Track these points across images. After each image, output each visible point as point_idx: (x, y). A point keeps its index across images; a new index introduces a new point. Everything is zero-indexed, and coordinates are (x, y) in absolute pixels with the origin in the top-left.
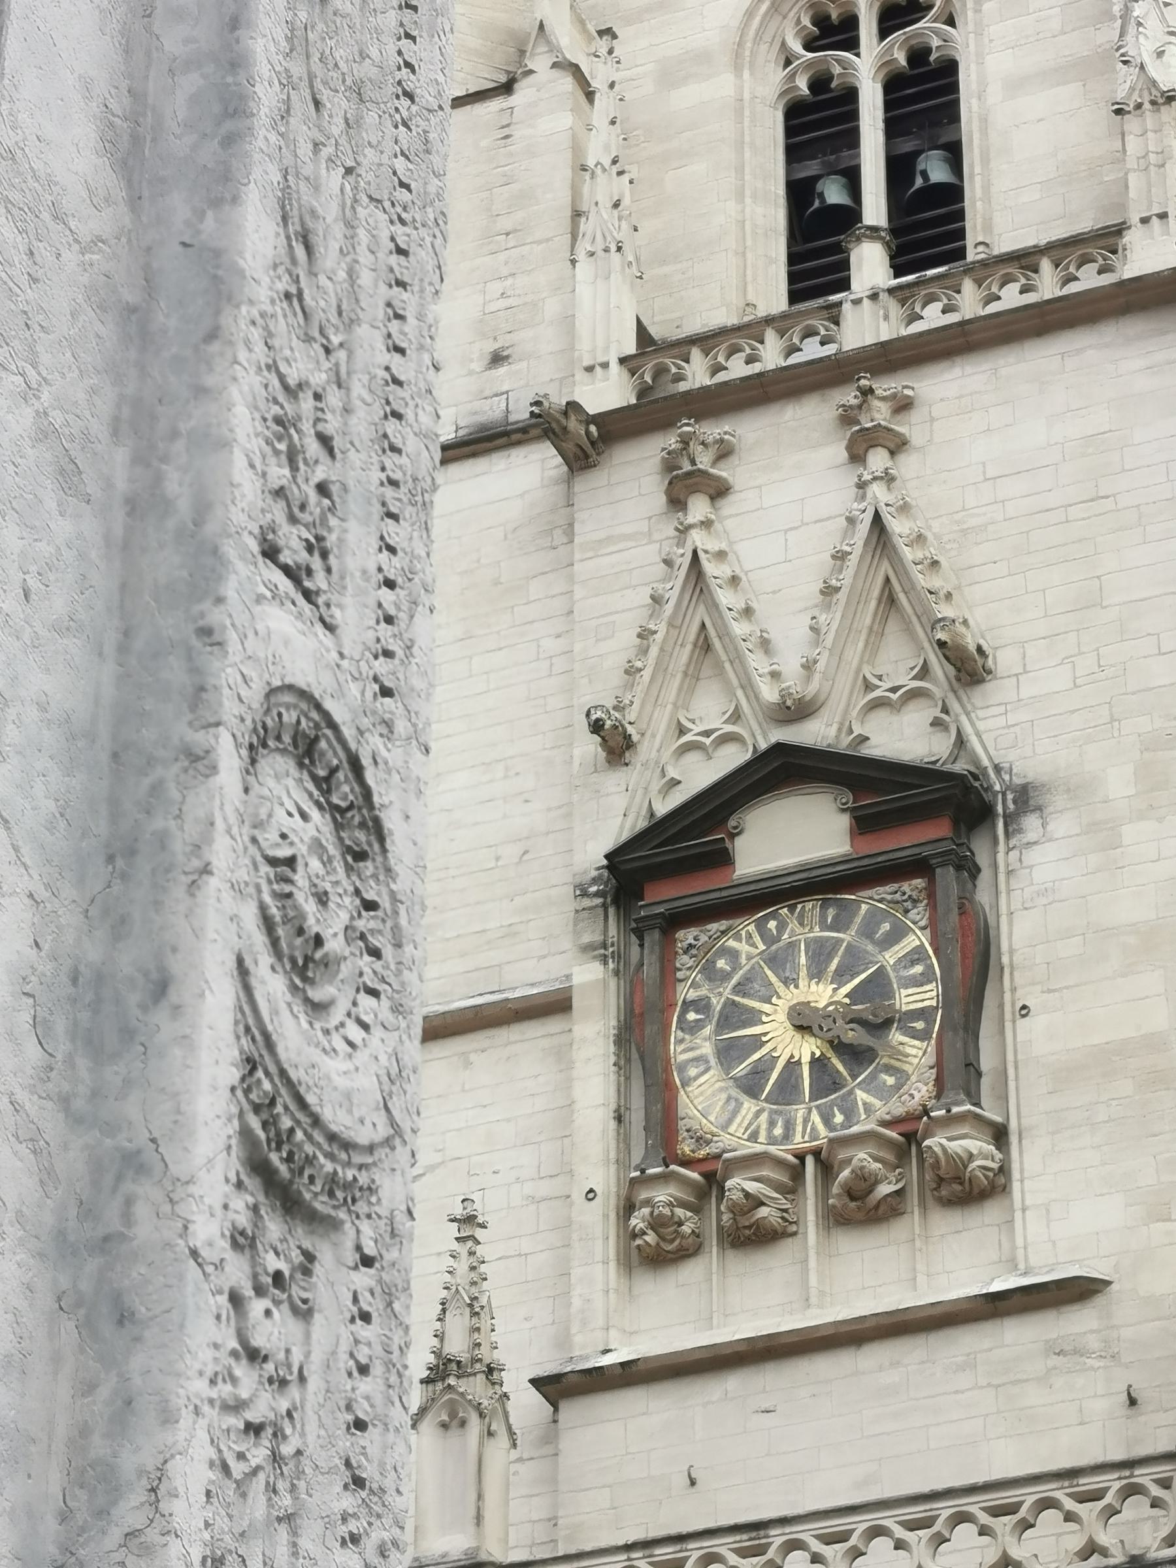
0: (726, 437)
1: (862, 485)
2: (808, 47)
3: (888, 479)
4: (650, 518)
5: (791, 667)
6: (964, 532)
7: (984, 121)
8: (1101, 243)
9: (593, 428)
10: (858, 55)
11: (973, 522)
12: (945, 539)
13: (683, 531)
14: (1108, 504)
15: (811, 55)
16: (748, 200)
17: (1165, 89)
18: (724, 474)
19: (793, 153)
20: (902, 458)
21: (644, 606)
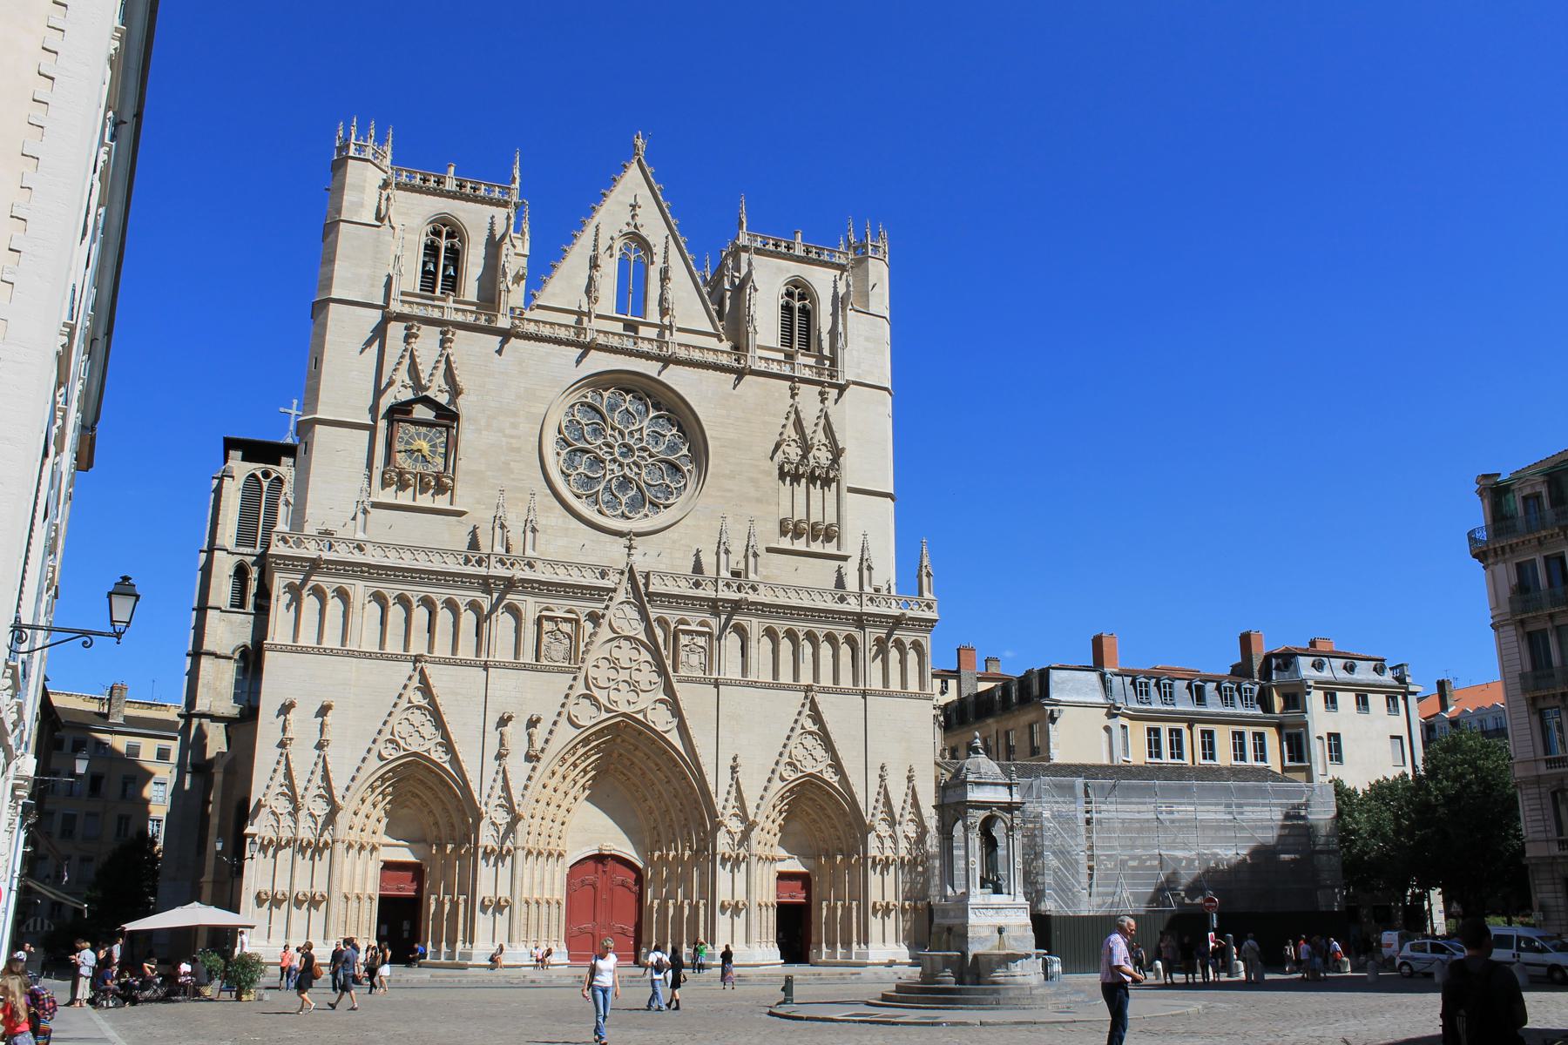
19: (425, 254)
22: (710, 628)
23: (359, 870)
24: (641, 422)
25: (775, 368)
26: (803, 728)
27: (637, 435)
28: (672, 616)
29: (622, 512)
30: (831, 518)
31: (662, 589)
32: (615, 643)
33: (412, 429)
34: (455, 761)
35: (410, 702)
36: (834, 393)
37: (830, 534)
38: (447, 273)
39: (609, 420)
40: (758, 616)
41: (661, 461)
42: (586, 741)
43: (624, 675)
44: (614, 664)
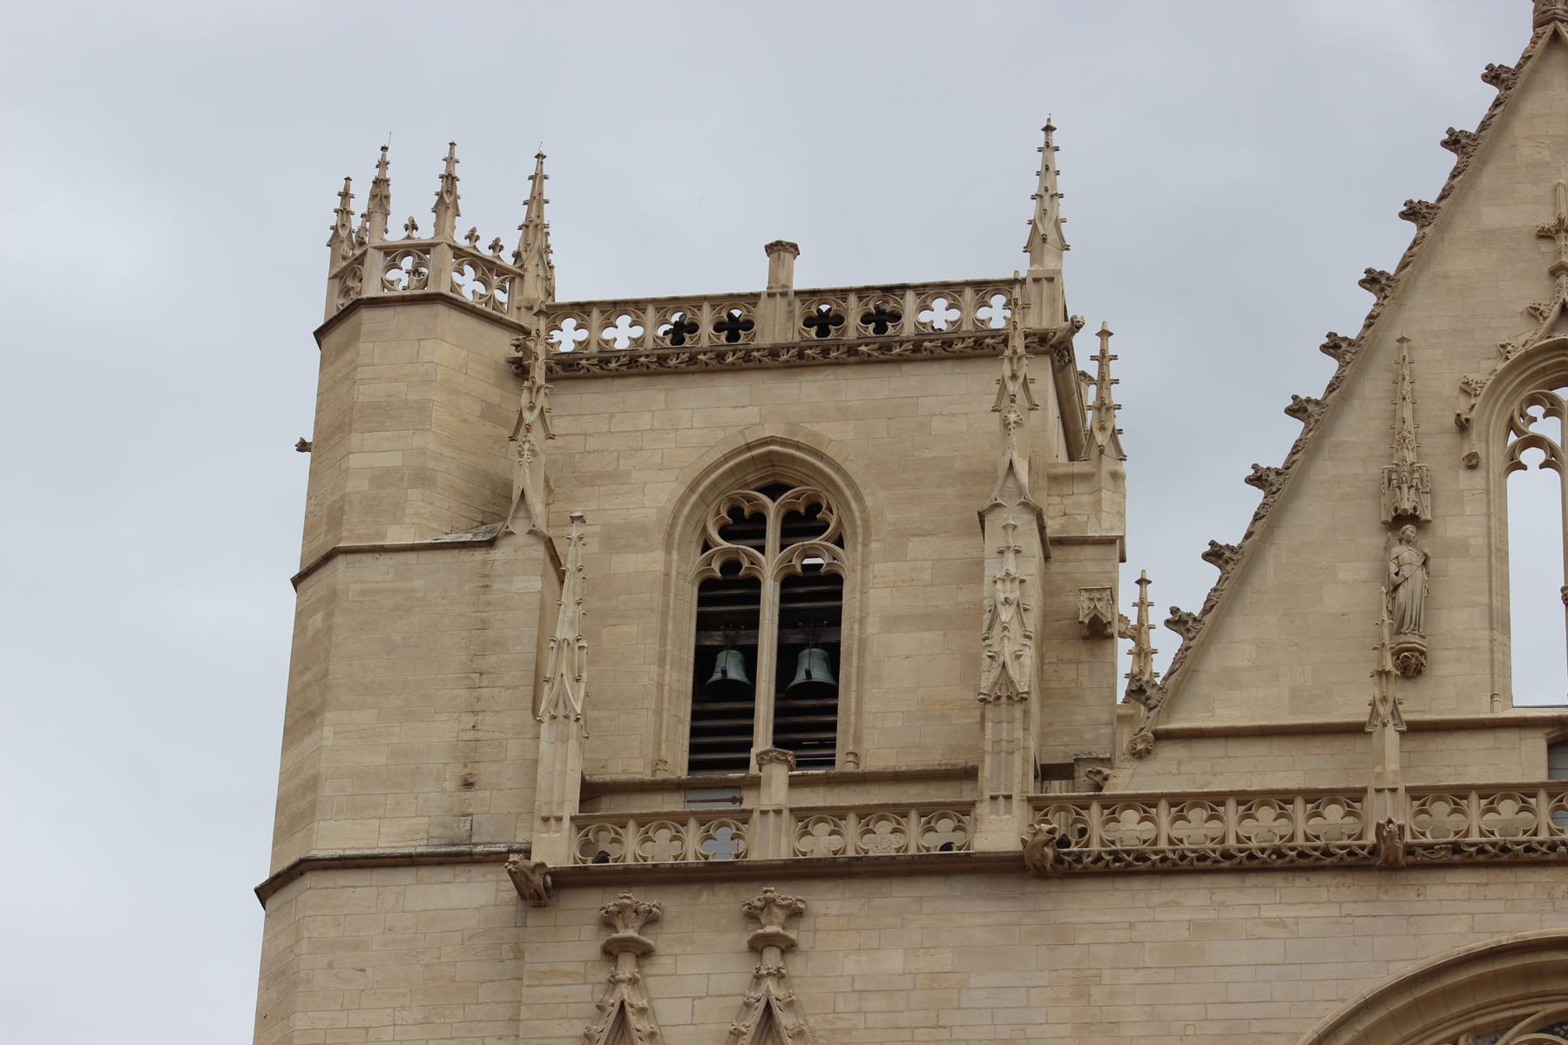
0: (654, 909)
1: (758, 978)
2: (725, 533)
3: (779, 976)
4: (586, 962)
6: (834, 1031)
7: (862, 643)
8: (958, 808)
9: (549, 879)
10: (762, 549)
11: (840, 1025)
12: (818, 1033)
13: (614, 983)
14: (945, 1034)
15: (726, 545)
16: (668, 667)
17: (1021, 691)
18: (650, 942)
19: (704, 623)
20: (790, 958)
21: (576, 1037)
38: (800, 677)
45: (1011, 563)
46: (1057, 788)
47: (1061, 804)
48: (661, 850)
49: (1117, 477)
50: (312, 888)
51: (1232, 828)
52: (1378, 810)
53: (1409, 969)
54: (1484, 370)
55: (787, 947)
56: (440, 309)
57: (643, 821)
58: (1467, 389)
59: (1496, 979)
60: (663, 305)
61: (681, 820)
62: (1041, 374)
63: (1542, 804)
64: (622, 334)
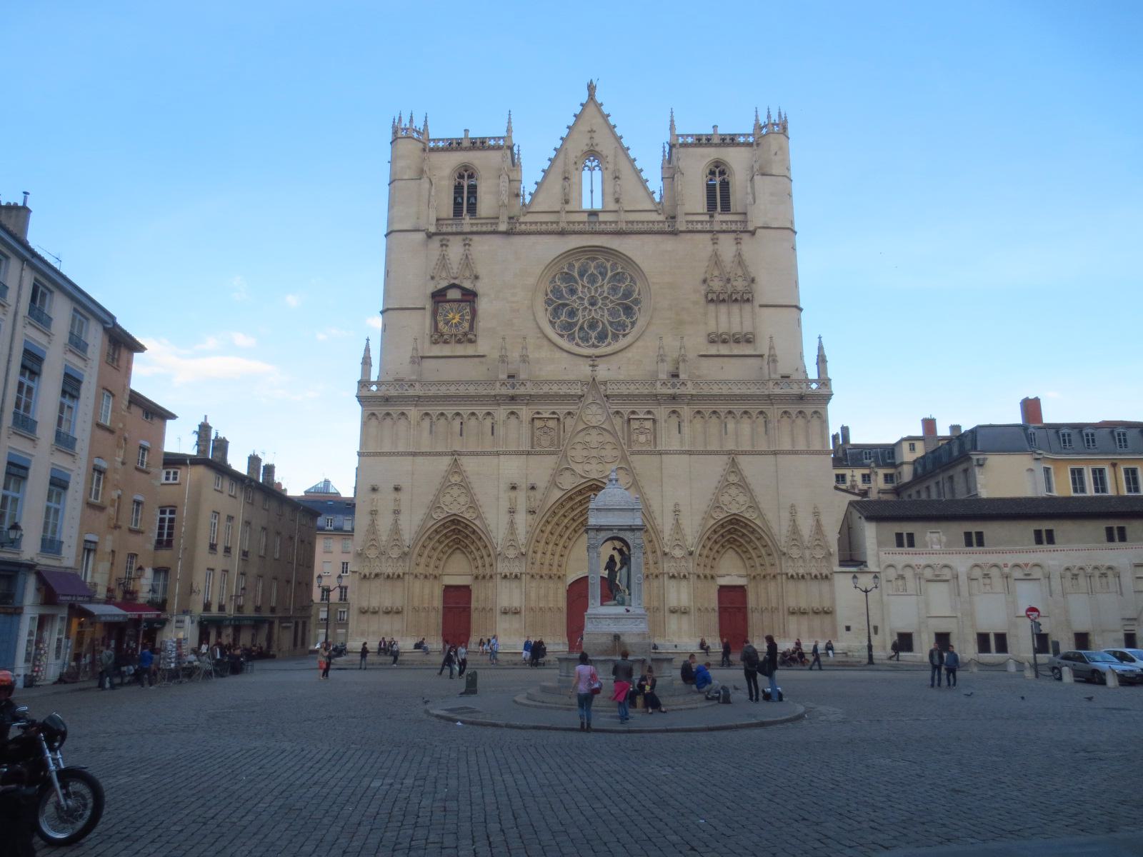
3: (469, 250)
5: (455, 271)
13: (442, 251)
19: (455, 193)
22: (654, 414)
23: (427, 591)
24: (603, 280)
25: (699, 227)
26: (727, 481)
27: (600, 290)
28: (626, 410)
29: (593, 343)
30: (747, 328)
31: (616, 392)
32: (584, 432)
33: (447, 306)
34: (479, 517)
35: (450, 481)
36: (745, 237)
37: (749, 341)
39: (580, 282)
40: (688, 404)
41: (618, 304)
42: (571, 498)
43: (594, 453)
44: (586, 446)
45: (504, 184)
46: (512, 221)
47: (512, 223)
48: (449, 230)
49: (521, 170)
50: (394, 235)
51: (539, 228)
52: (561, 225)
53: (566, 250)
54: (579, 154)
55: (469, 245)
56: (411, 139)
57: (446, 224)
58: (576, 157)
59: (582, 252)
60: (447, 140)
61: (453, 225)
62: (509, 152)
63: (587, 224)
64: (441, 144)
